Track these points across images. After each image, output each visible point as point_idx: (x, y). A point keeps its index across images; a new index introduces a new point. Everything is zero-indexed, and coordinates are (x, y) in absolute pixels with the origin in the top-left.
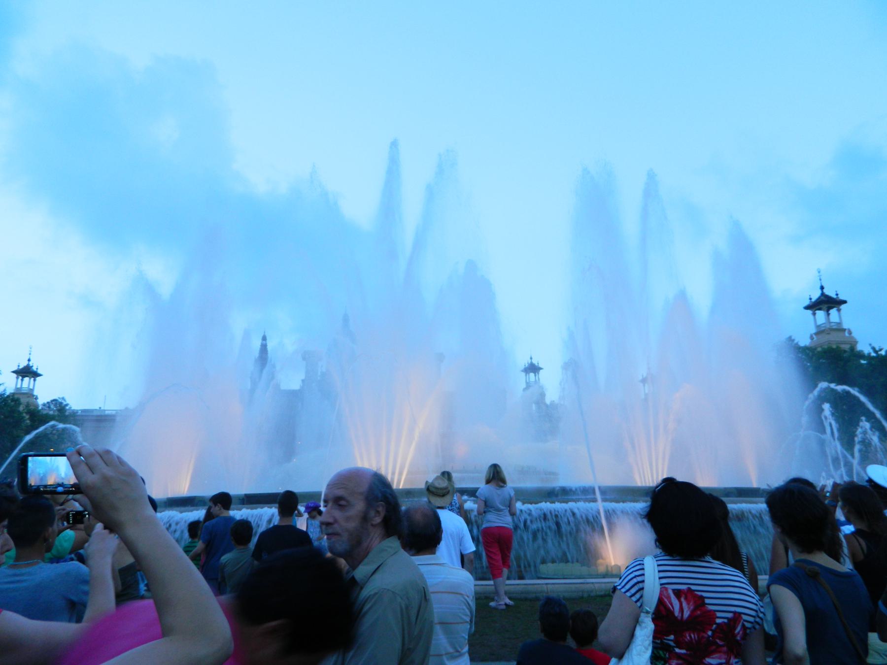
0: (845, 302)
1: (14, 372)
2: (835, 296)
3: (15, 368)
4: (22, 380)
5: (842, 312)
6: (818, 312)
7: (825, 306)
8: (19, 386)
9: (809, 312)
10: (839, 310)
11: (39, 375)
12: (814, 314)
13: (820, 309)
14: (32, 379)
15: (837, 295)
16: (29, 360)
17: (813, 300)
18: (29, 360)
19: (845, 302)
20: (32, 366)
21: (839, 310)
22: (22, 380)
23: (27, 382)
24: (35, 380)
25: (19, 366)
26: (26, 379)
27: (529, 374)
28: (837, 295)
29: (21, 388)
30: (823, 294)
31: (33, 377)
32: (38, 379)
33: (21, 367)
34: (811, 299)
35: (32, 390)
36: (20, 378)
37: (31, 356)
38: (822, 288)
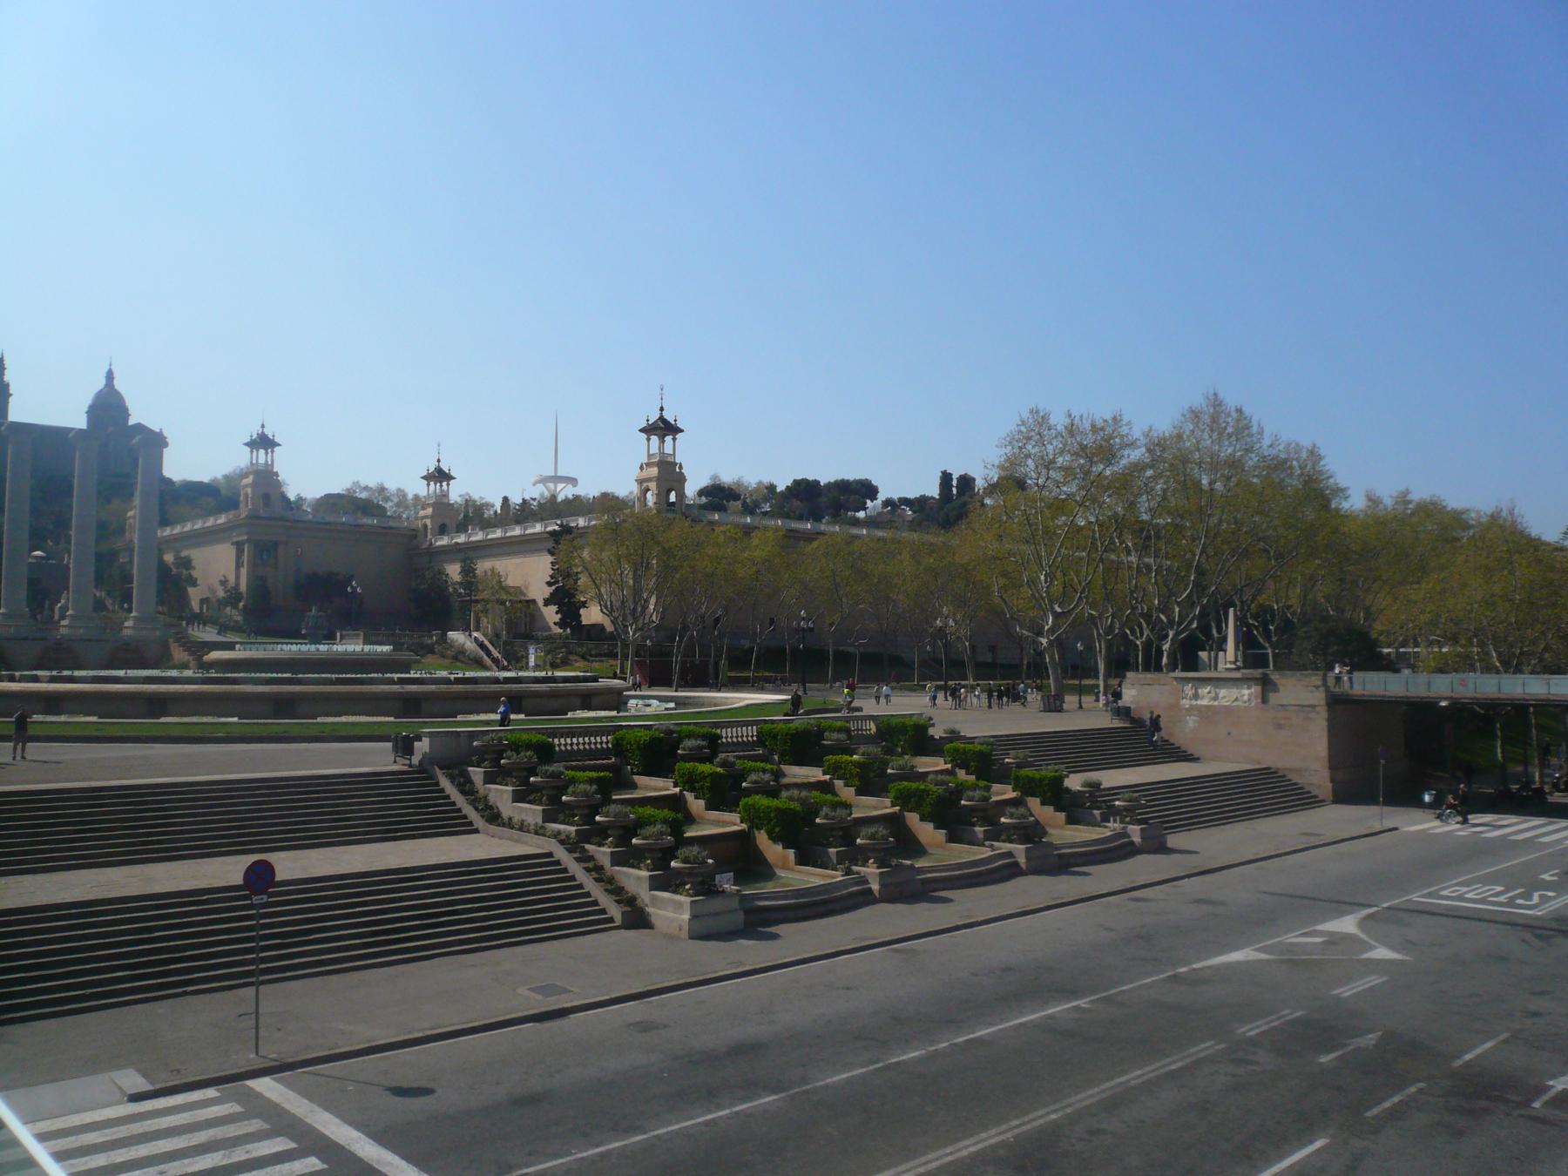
0: (682, 431)
2: (673, 423)
5: (677, 442)
6: (652, 437)
7: (658, 432)
9: (644, 436)
10: (674, 439)
12: (648, 440)
13: (655, 435)
15: (675, 421)
17: (650, 423)
19: (682, 431)
21: (674, 439)
27: (258, 451)
28: (675, 421)
30: (662, 419)
34: (648, 420)
38: (662, 409)
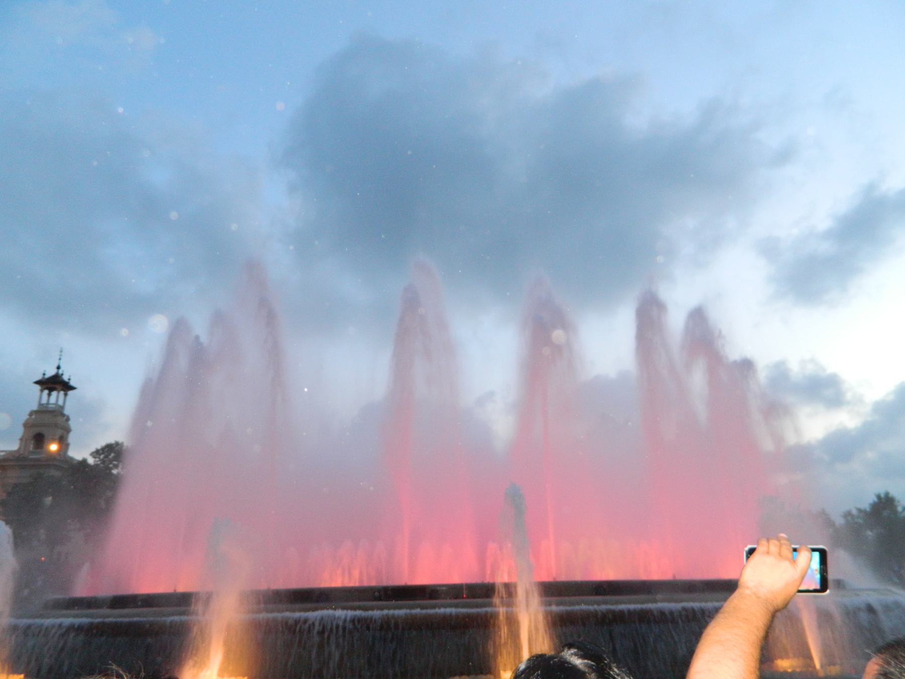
1: (37, 383)
3: (39, 377)
4: (49, 395)
8: (44, 401)
11: (72, 388)
14: (62, 393)
16: (58, 368)
18: (58, 368)
20: (62, 375)
22: (49, 395)
23: (56, 397)
24: (66, 395)
25: (44, 374)
26: (54, 394)
29: (48, 403)
31: (62, 390)
32: (70, 393)
33: (47, 376)
35: (62, 407)
36: (46, 392)
37: (62, 361)
